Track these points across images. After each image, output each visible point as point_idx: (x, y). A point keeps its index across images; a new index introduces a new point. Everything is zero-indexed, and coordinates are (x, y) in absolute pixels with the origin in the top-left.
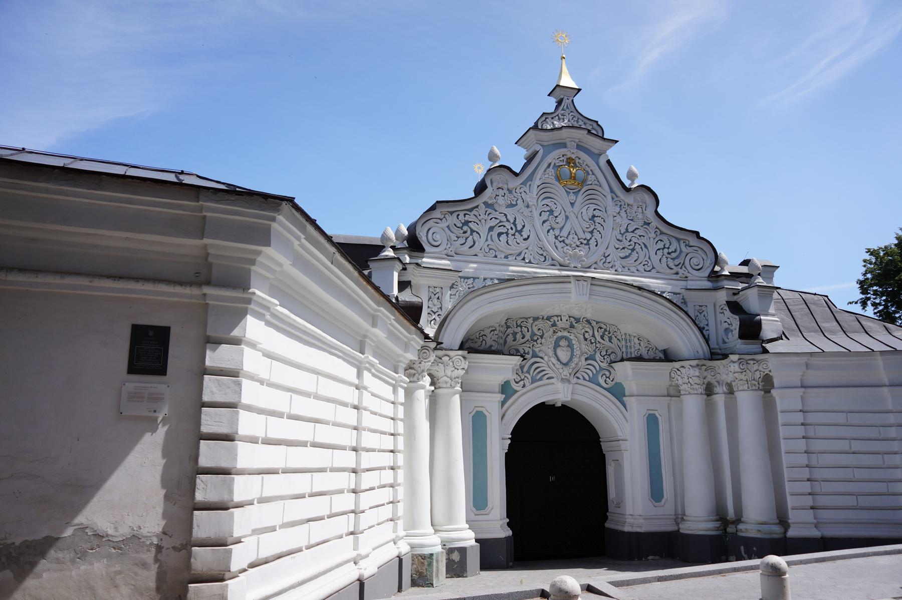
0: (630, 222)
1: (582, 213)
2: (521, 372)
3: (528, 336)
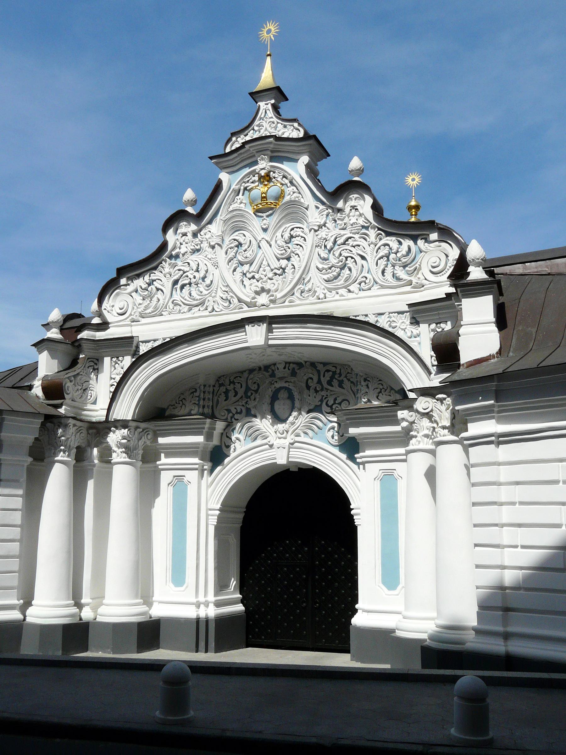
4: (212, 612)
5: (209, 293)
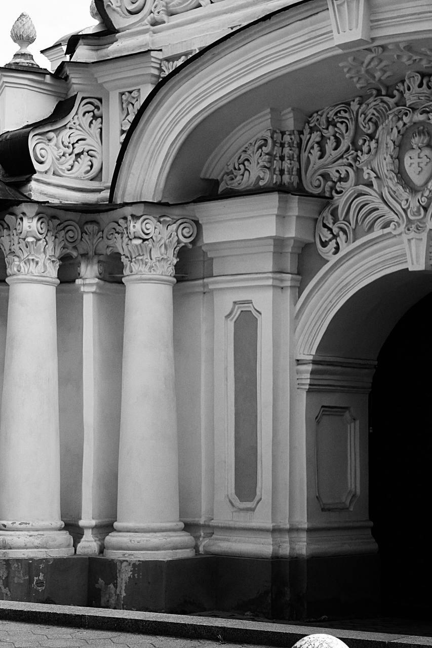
2: (331, 221)
3: (345, 143)
4: (303, 547)
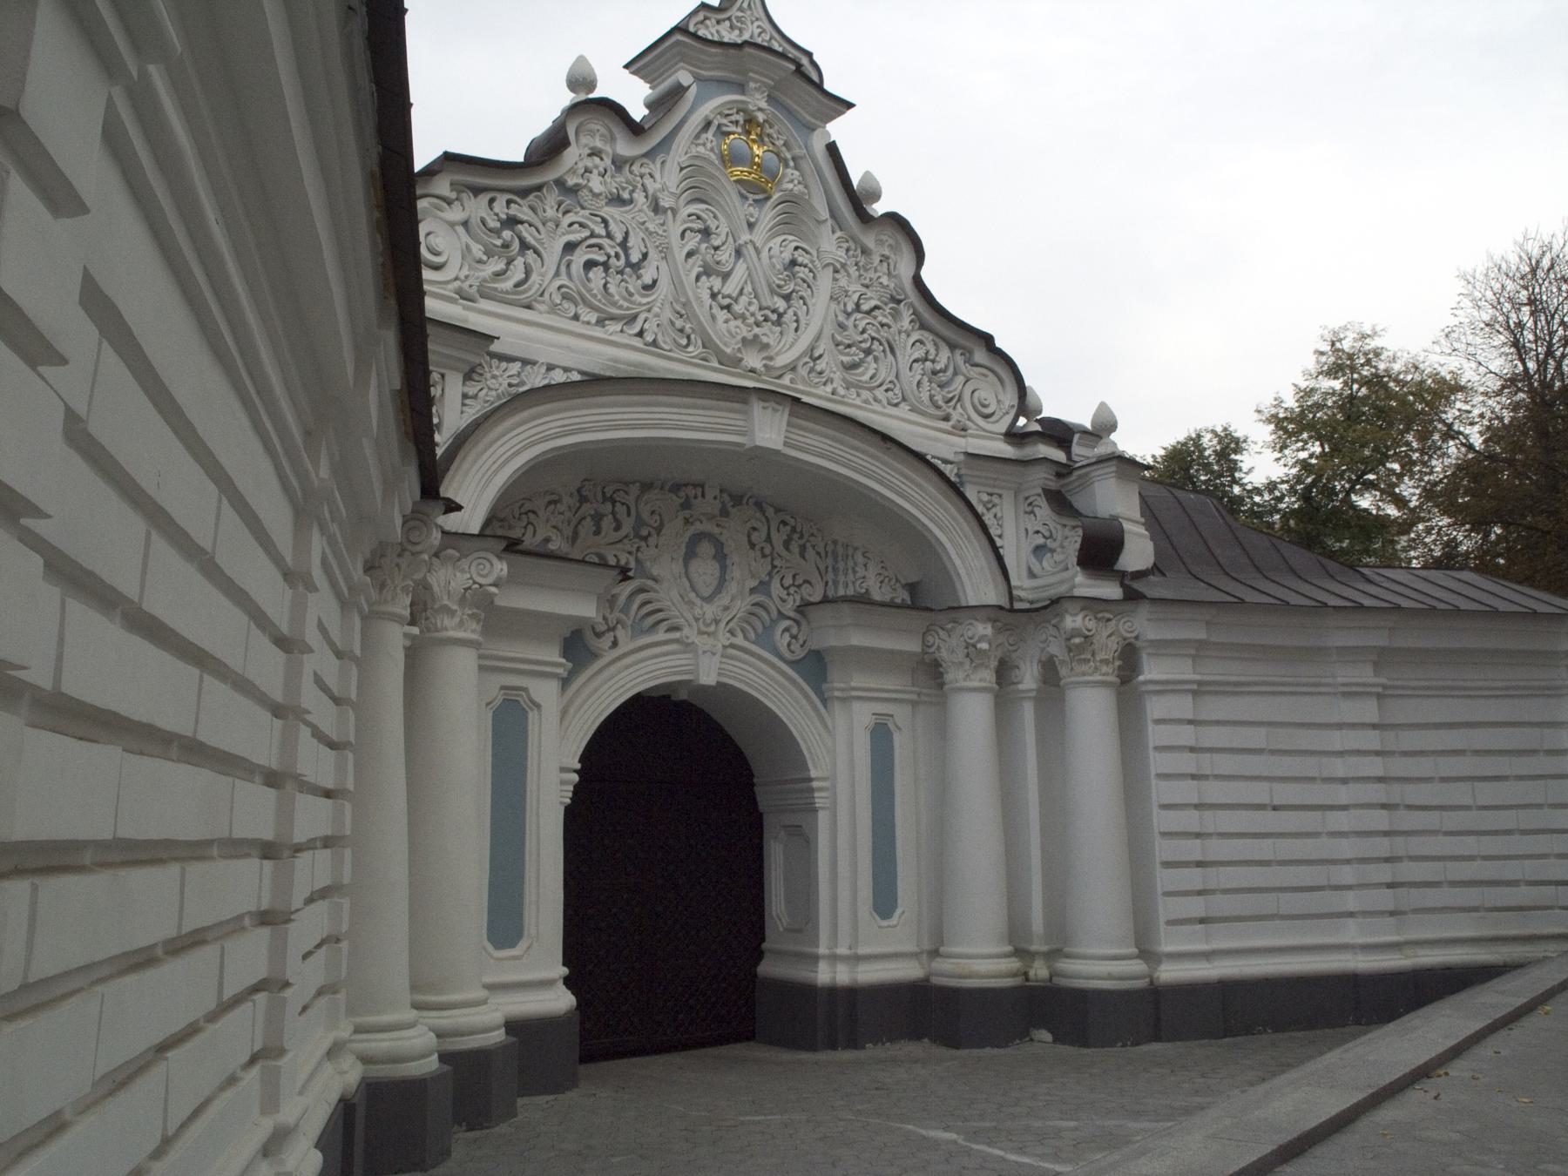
0: (864, 290)
1: (769, 250)
3: (627, 528)
5: (648, 303)
